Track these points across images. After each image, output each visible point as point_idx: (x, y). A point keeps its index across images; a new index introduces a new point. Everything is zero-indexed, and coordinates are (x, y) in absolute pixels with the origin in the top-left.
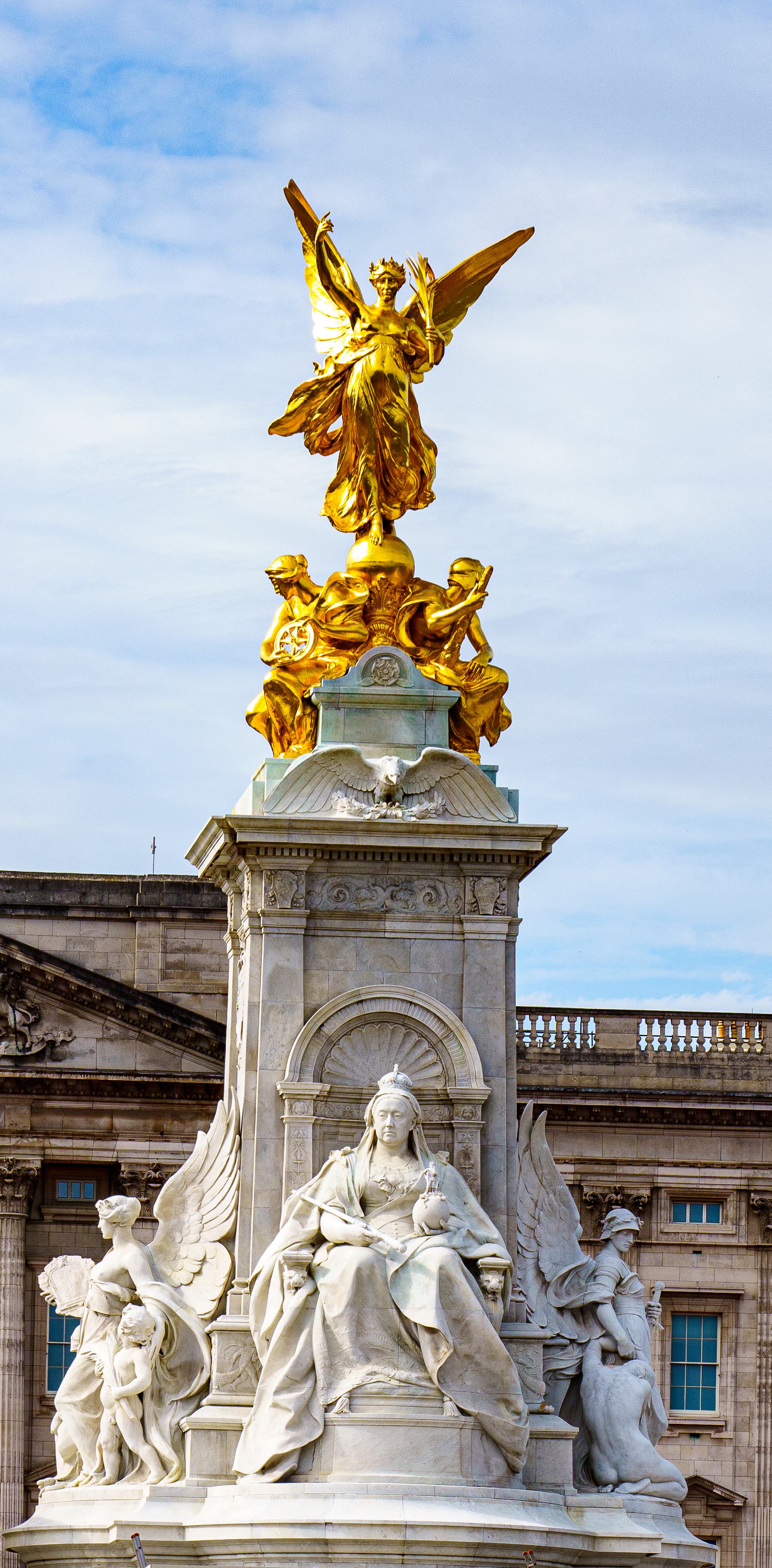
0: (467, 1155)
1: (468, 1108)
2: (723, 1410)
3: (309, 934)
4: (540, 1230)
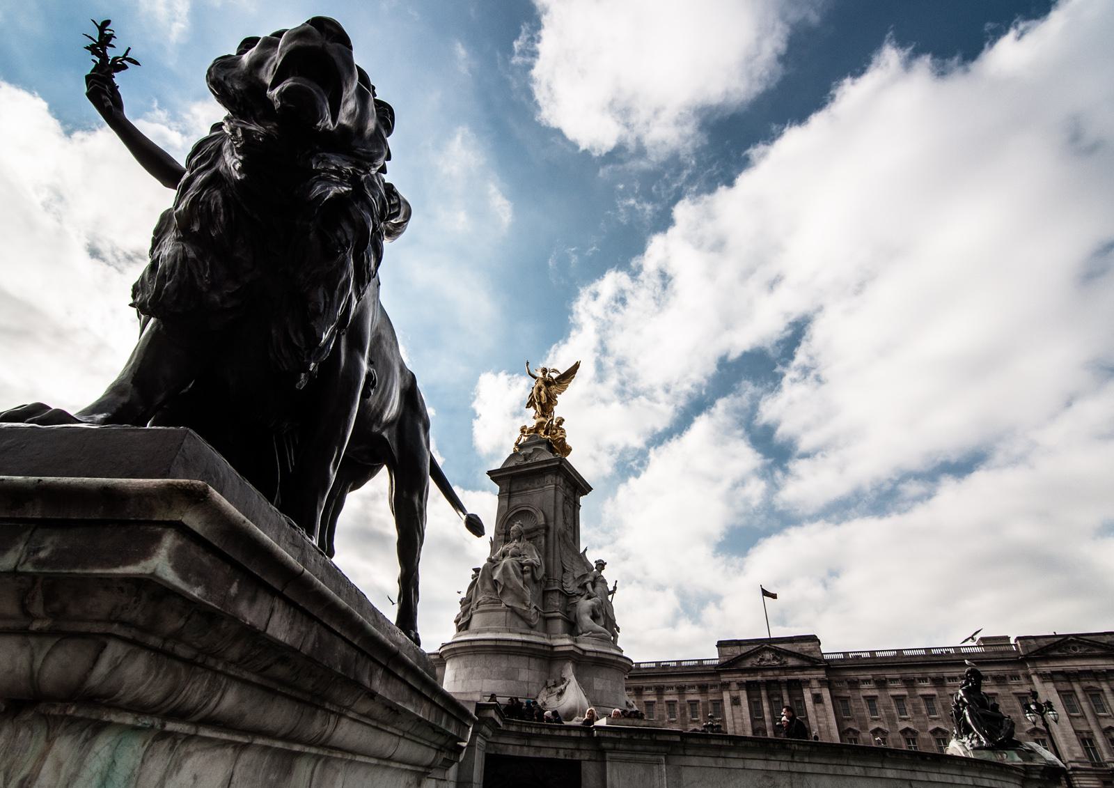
0: (540, 542)
1: (541, 531)
2: (909, 716)
3: (510, 497)
4: (574, 567)
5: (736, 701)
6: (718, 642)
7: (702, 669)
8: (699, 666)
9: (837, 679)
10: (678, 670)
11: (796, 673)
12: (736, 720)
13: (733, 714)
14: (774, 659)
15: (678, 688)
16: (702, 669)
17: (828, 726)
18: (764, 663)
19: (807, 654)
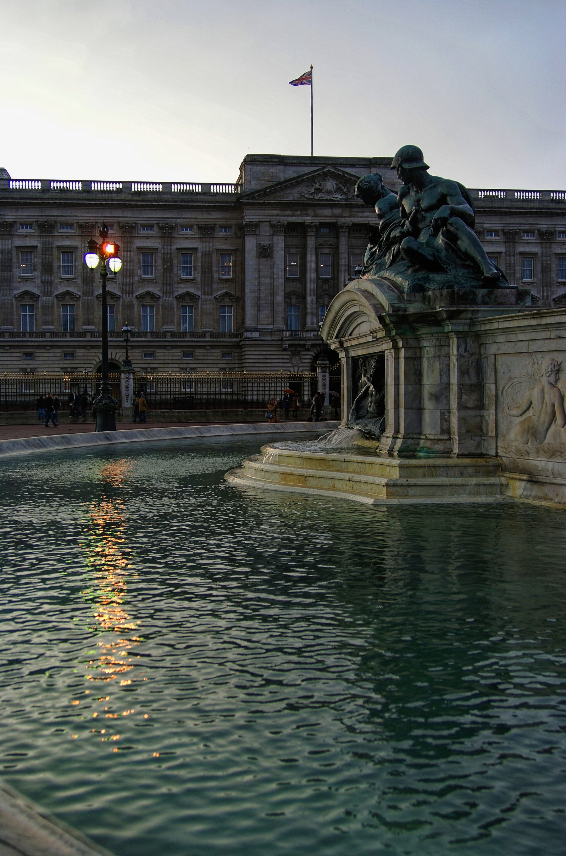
5: (265, 252)
6: (248, 156)
7: (209, 198)
8: (203, 193)
10: (165, 197)
11: (365, 214)
12: (262, 280)
13: (258, 271)
14: (339, 190)
15: (161, 228)
16: (209, 198)
18: (320, 195)
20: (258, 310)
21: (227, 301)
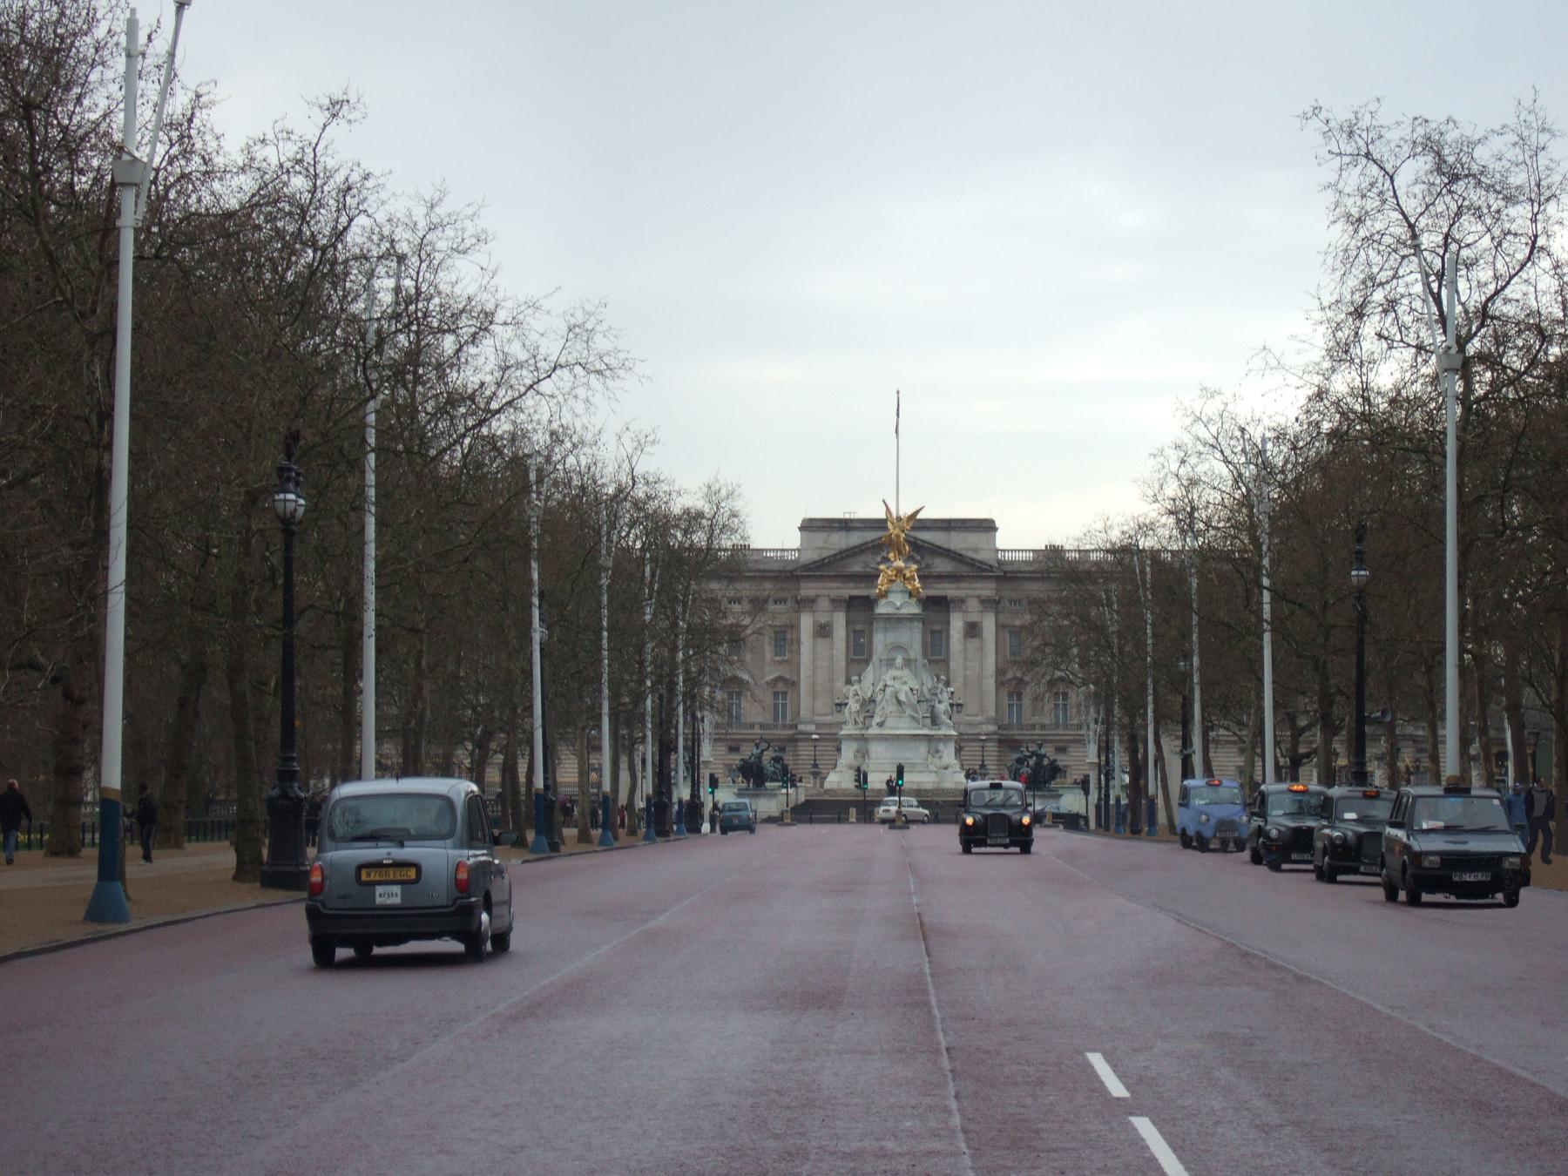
5: (823, 631)
9: (1013, 595)
13: (814, 652)
17: (981, 676)
19: (970, 554)
20: (814, 698)
21: (781, 687)
